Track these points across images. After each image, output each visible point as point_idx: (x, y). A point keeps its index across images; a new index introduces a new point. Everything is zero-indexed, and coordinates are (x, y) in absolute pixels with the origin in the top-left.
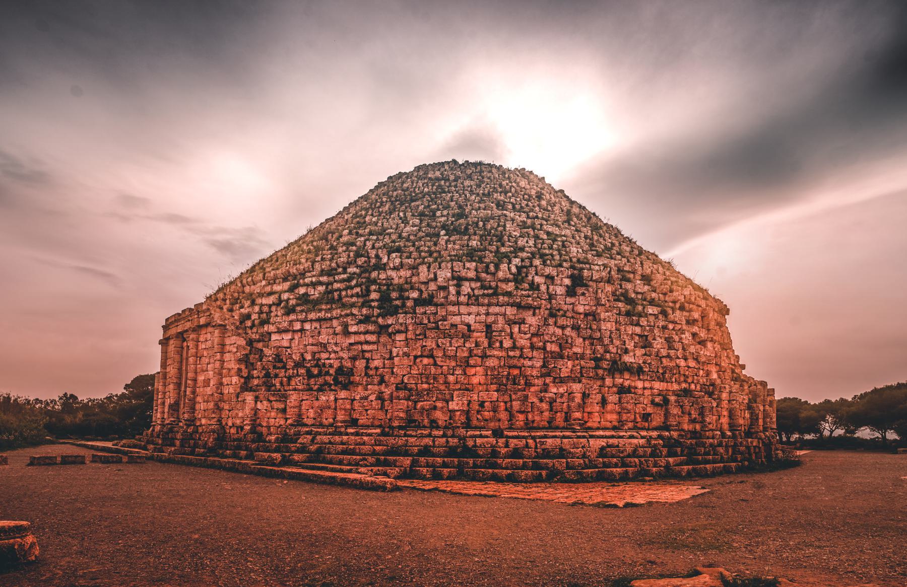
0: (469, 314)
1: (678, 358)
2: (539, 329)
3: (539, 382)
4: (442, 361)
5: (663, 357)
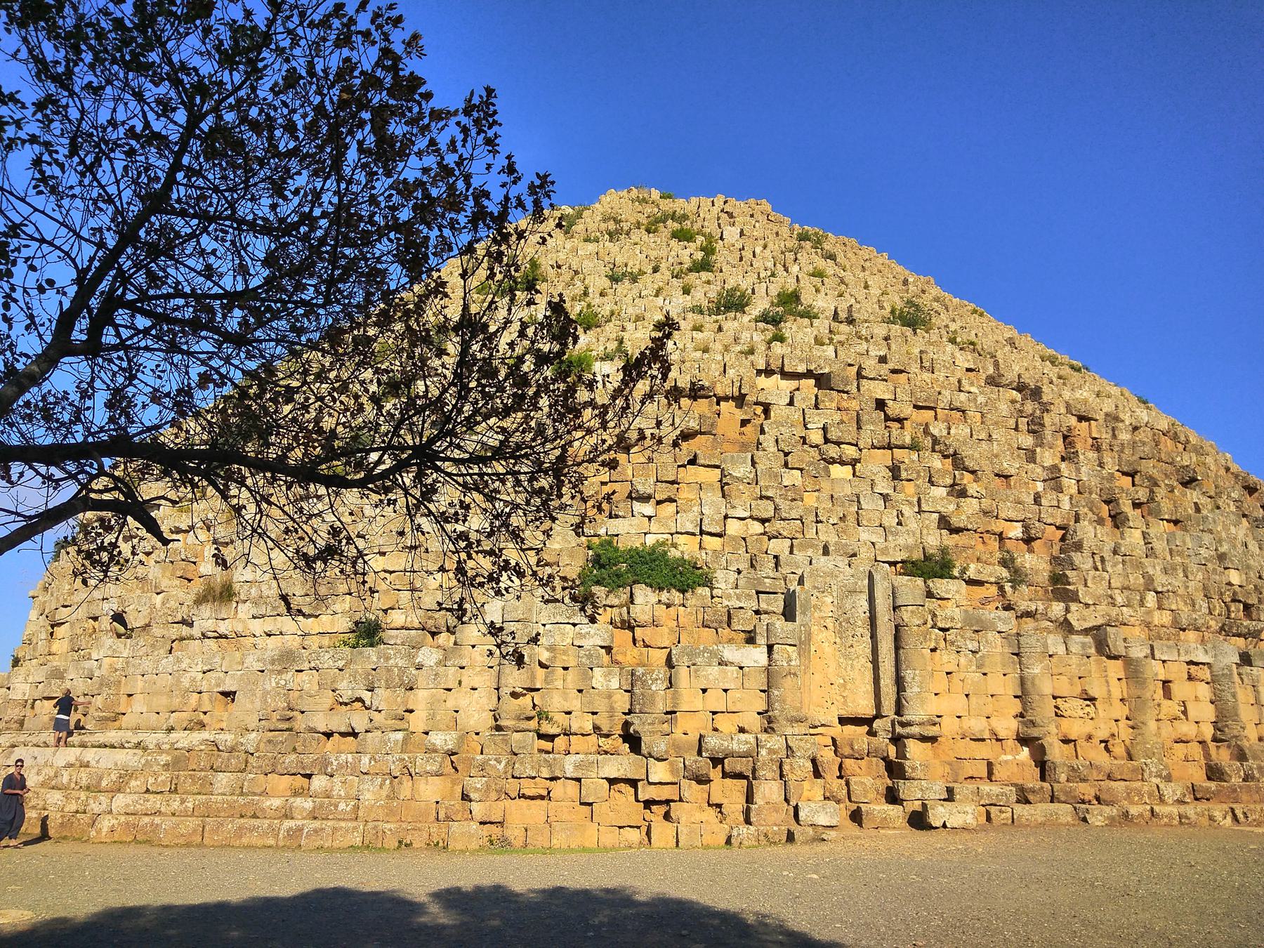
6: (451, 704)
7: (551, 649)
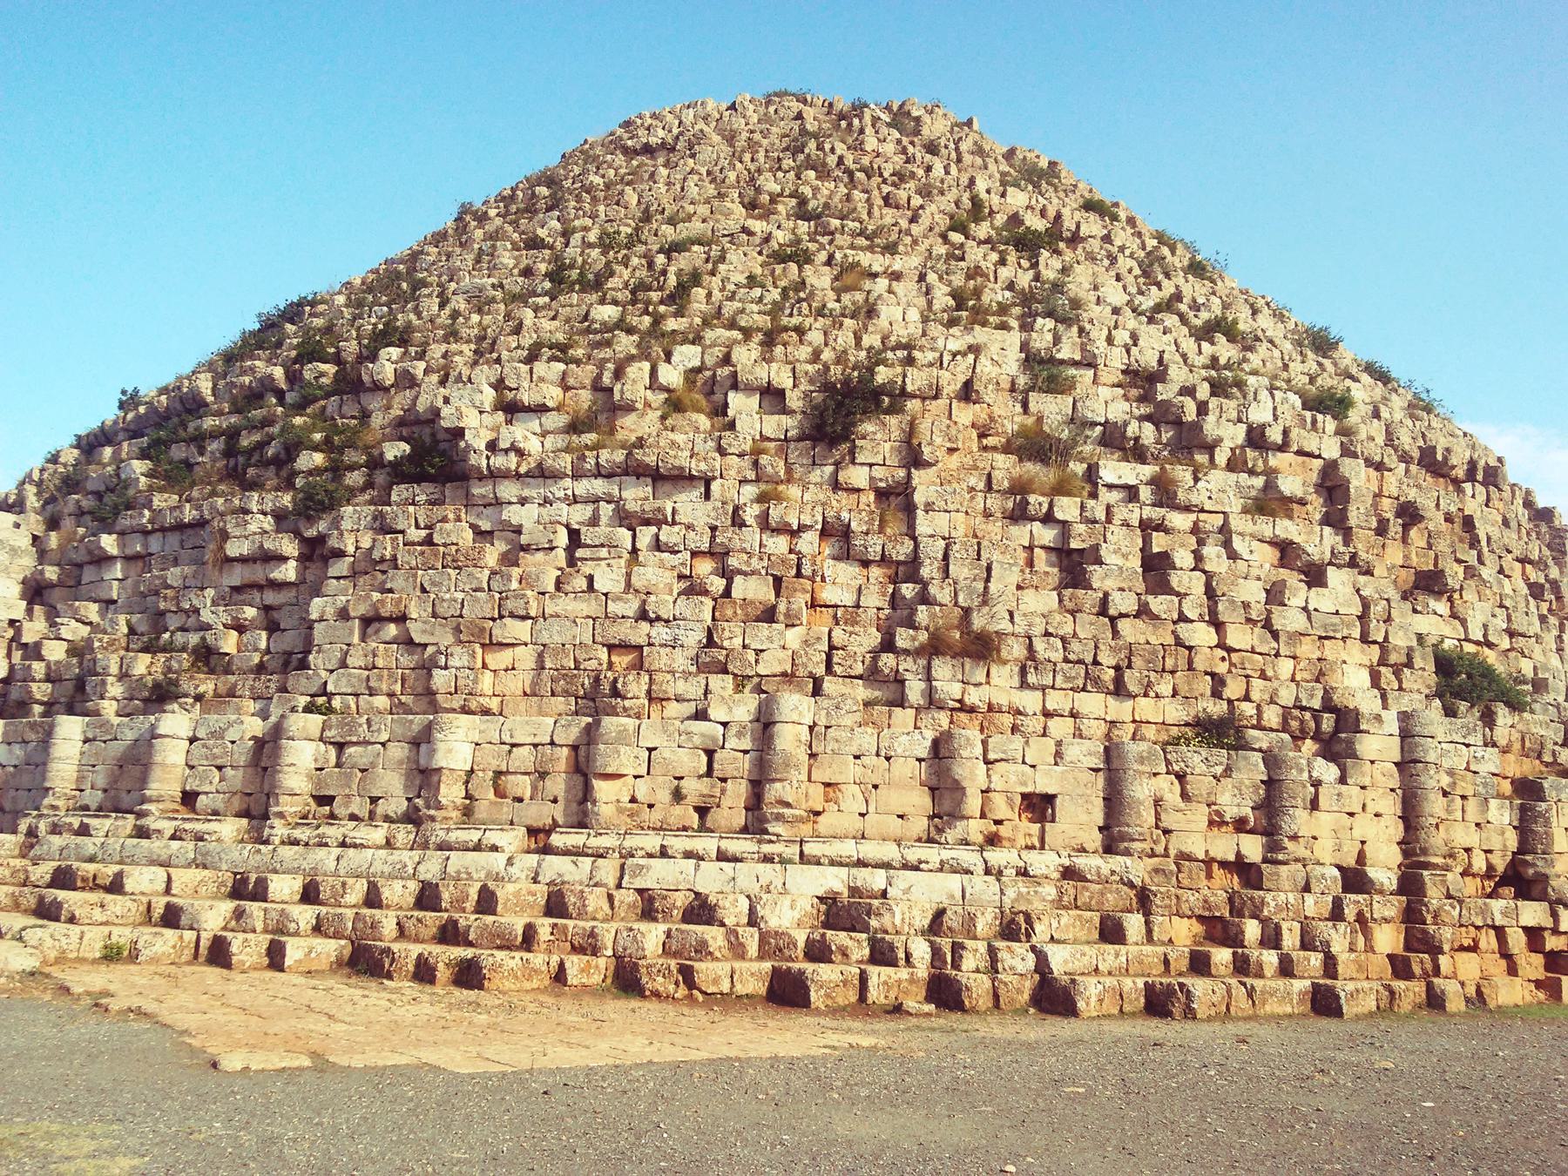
0: (523, 501)
1: (1182, 618)
2: (713, 537)
3: (693, 688)
4: (424, 632)
5: (1122, 615)
6: (1358, 834)
7: (1451, 773)
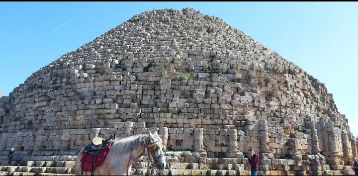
6: (249, 145)
